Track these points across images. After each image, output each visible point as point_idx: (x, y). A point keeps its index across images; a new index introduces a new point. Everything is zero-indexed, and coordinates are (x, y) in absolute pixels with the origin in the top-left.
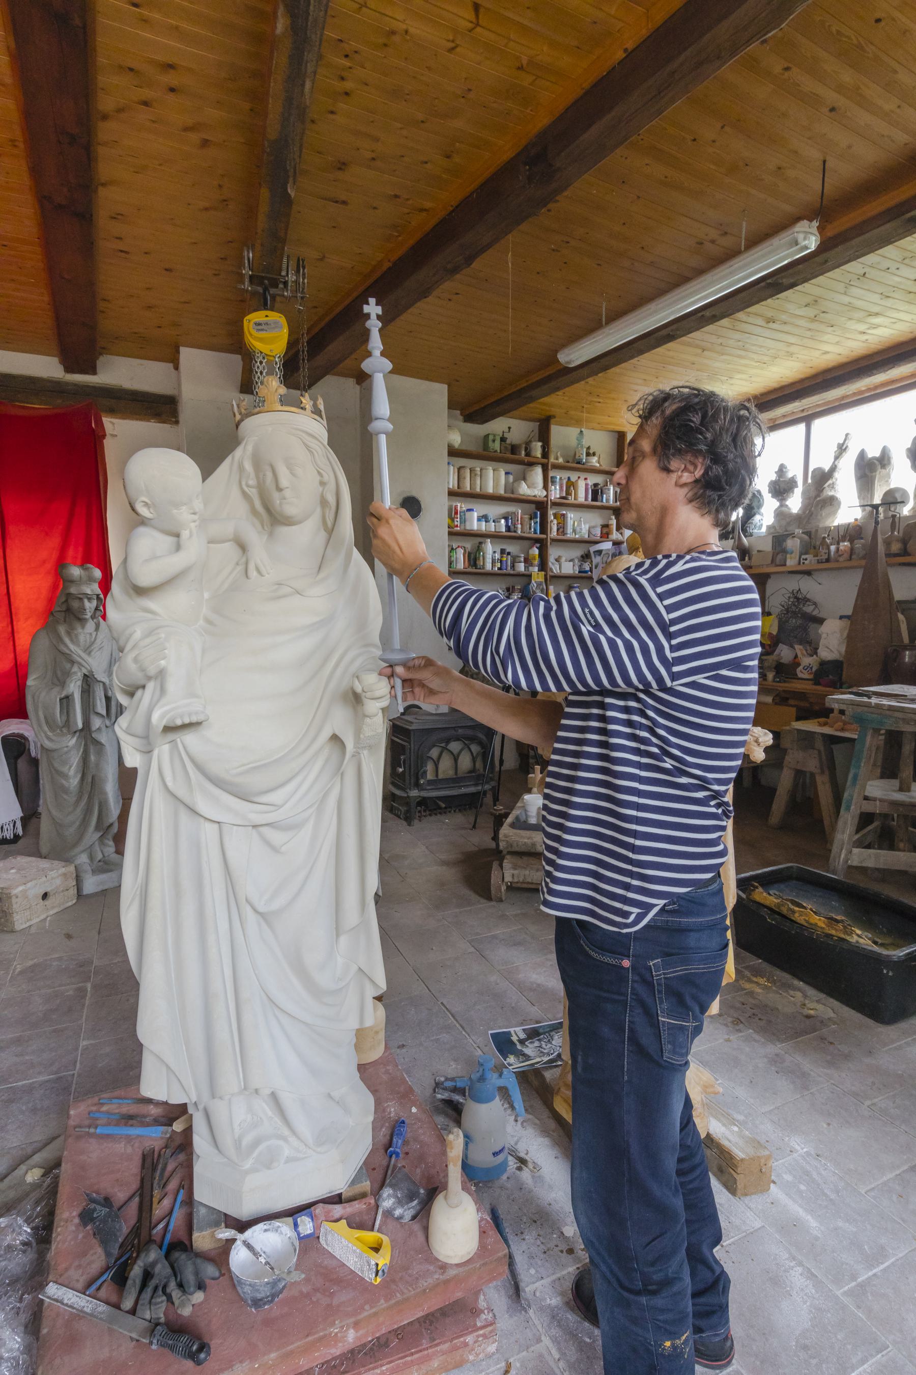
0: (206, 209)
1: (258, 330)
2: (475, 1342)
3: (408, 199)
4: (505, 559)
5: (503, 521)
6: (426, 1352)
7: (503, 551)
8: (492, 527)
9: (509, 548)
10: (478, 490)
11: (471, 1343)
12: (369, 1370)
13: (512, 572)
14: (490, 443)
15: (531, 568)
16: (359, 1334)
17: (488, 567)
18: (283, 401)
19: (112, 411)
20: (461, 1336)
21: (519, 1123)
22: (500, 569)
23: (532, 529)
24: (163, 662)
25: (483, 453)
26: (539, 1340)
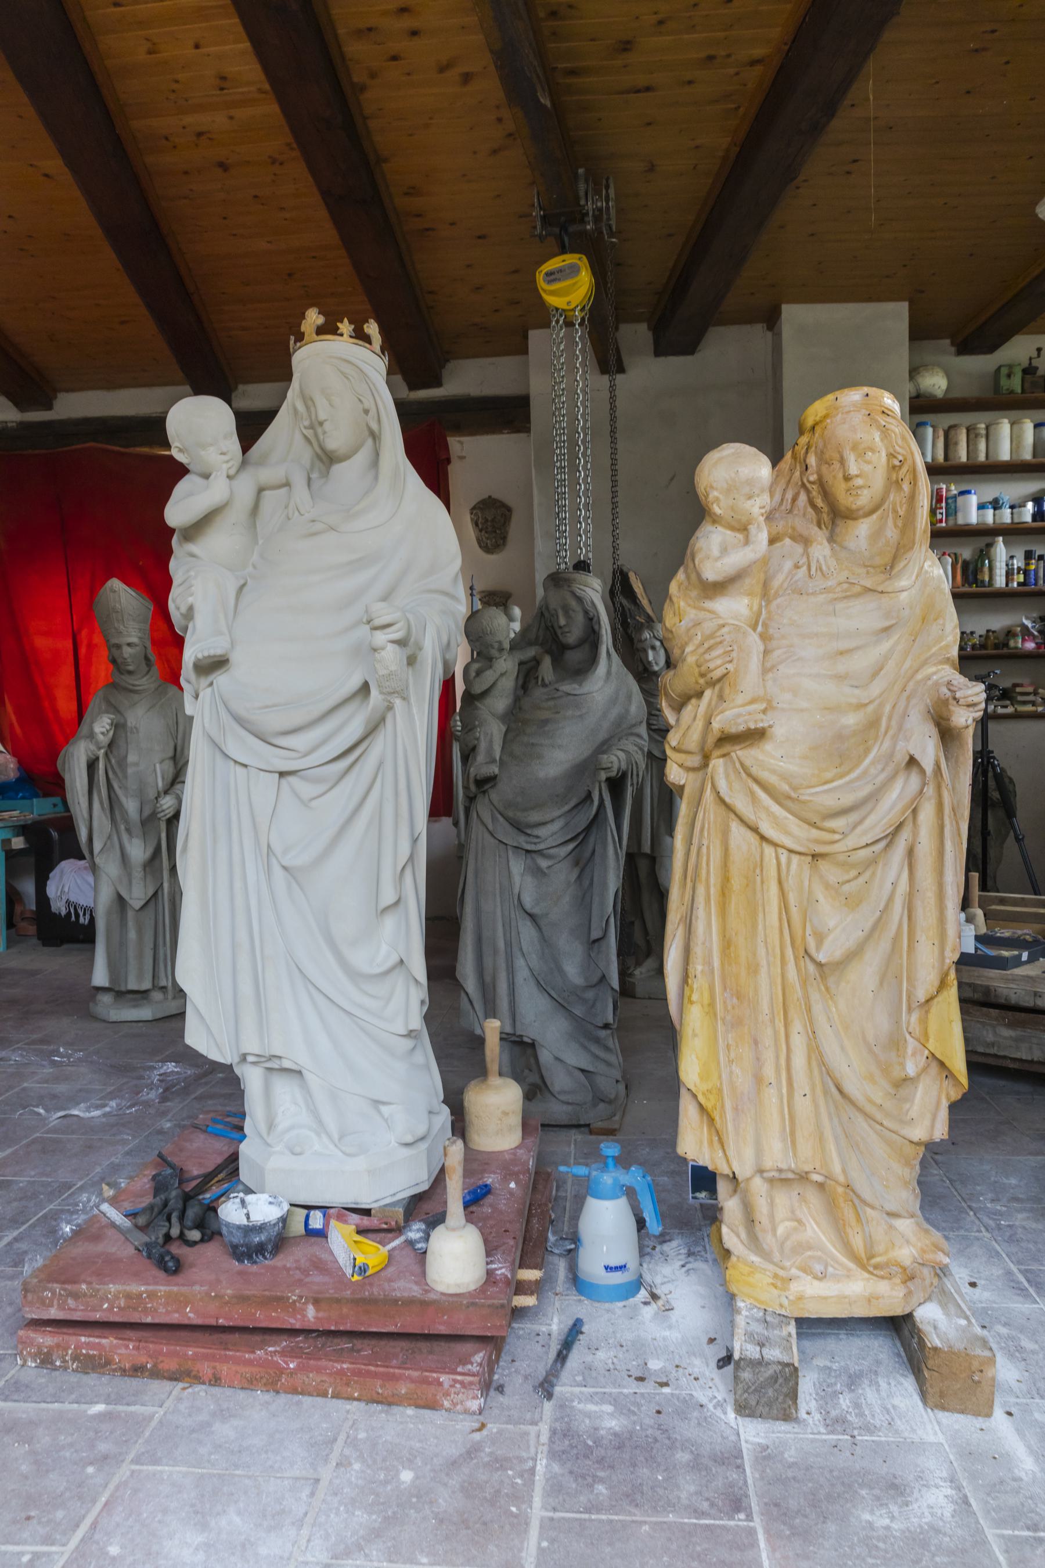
0: (495, 152)
1: (549, 282)
2: (452, 1386)
3: (729, 56)
4: (1033, 567)
5: (1030, 505)
6: (392, 1370)
7: (1028, 555)
8: (1006, 516)
10: (982, 457)
11: (446, 1386)
12: (330, 1360)
14: (1004, 382)
16: (321, 1315)
17: (1000, 582)
18: (321, 331)
19: (459, 429)
20: (435, 1372)
21: (684, 1269)
22: (1019, 584)
24: (190, 600)
25: (996, 400)
26: (534, 1423)
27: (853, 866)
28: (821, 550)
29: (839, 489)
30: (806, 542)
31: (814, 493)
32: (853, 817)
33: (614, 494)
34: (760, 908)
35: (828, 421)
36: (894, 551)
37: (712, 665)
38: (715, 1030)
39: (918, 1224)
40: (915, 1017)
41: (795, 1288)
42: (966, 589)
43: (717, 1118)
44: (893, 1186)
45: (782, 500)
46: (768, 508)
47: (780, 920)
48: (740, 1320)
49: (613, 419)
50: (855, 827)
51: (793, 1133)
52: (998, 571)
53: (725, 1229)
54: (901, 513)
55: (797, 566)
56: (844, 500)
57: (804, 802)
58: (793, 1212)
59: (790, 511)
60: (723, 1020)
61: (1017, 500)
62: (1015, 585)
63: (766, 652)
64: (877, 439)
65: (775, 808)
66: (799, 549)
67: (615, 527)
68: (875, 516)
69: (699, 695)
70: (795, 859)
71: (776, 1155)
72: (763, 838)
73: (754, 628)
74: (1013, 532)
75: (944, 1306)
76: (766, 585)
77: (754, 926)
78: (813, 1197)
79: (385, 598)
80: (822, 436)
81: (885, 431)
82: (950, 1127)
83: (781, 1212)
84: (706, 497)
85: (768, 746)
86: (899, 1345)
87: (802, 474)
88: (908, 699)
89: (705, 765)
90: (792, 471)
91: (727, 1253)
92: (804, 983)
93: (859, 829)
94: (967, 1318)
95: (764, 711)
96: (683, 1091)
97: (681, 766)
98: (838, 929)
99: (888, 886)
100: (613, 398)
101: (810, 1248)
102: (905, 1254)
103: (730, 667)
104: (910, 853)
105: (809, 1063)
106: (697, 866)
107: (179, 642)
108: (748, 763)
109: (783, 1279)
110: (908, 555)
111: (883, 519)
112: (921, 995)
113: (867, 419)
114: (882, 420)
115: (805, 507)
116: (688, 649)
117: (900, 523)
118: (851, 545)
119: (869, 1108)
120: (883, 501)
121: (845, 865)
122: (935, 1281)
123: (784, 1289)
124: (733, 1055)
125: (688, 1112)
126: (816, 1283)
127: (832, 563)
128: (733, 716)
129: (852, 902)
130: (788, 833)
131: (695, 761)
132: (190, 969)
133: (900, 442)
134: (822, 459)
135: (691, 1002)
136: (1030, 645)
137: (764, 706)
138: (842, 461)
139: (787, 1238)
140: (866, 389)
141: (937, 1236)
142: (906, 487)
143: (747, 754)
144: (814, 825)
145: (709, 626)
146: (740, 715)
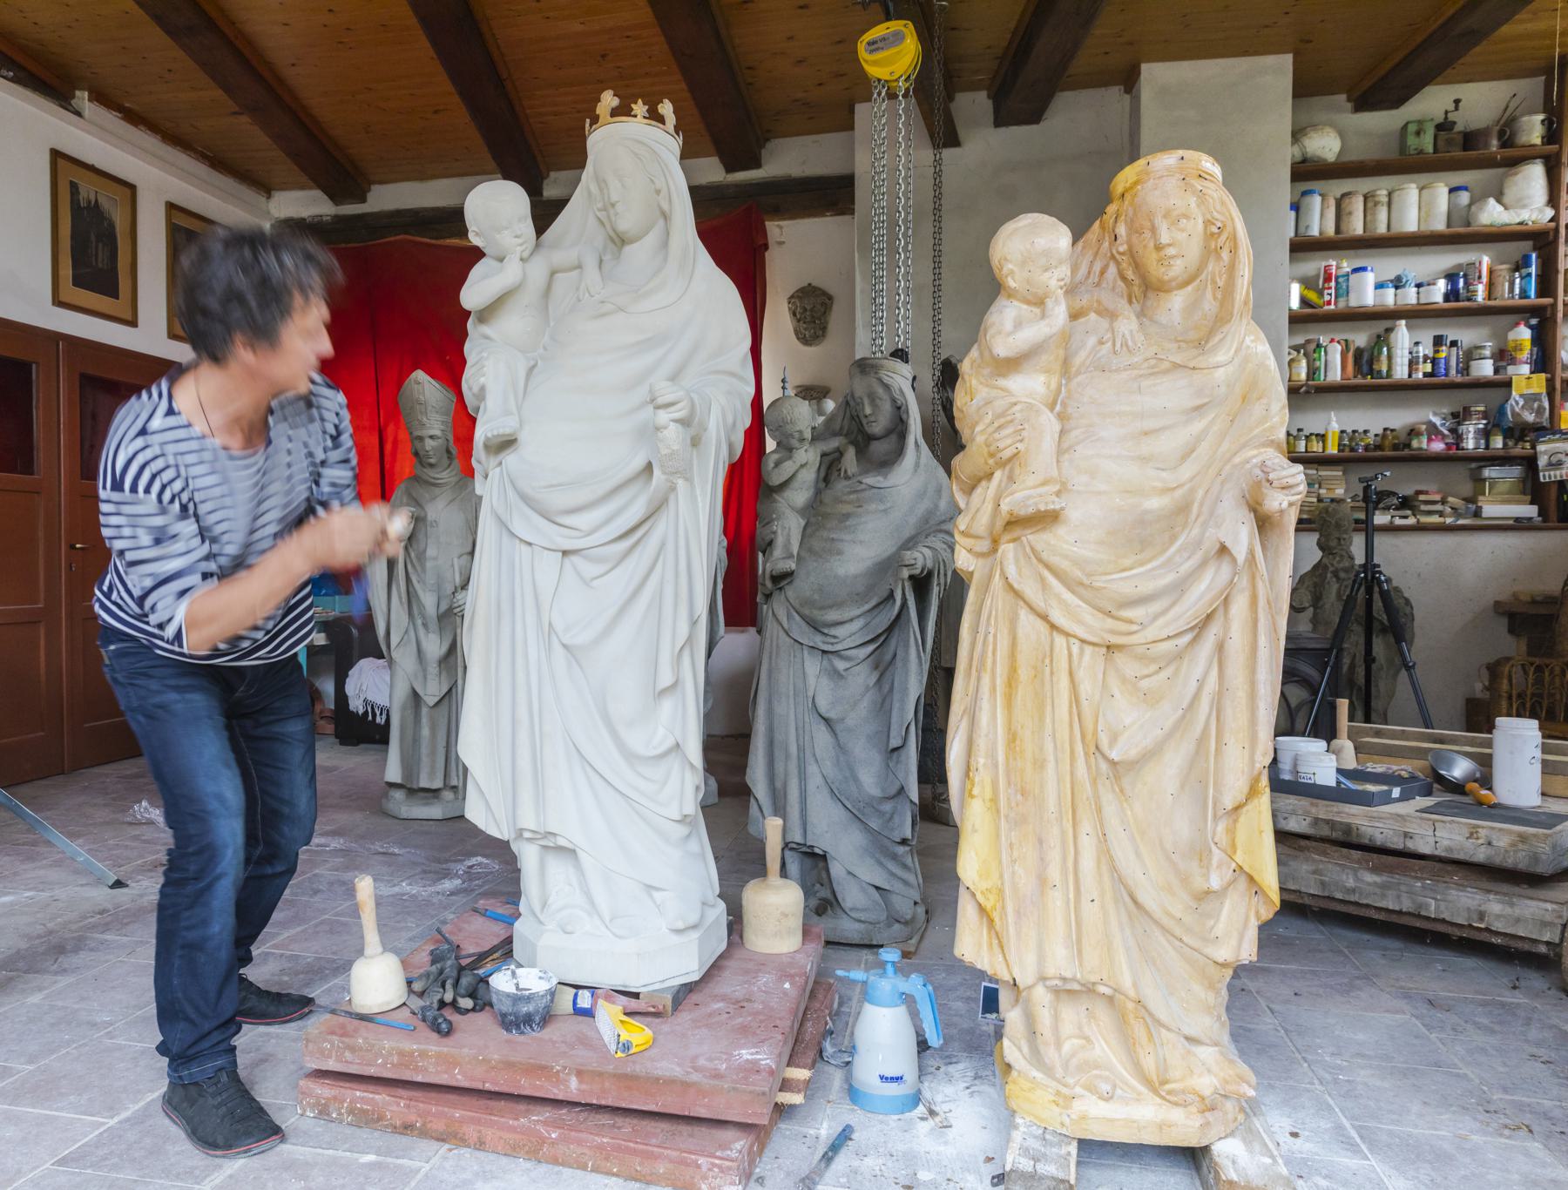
4: (1443, 355)
5: (1442, 285)
7: (1438, 341)
9: (1451, 334)
13: (1459, 379)
15: (1511, 370)
22: (1426, 375)
23: (1519, 288)
27: (1153, 660)
28: (1128, 324)
29: (1151, 259)
30: (1112, 315)
31: (1124, 265)
32: (1155, 607)
33: (937, 276)
34: (1049, 701)
37: (1001, 445)
38: (998, 829)
39: (1222, 1053)
40: (1221, 827)
41: (1078, 1106)
42: (1359, 381)
43: (997, 920)
44: (1196, 1010)
46: (1068, 280)
47: (1071, 713)
48: (1017, 1136)
49: (938, 197)
50: (1156, 617)
51: (1079, 941)
52: (1399, 360)
53: (1006, 1042)
54: (1220, 284)
55: (1101, 343)
56: (1155, 271)
57: (1098, 589)
58: (1080, 1028)
59: (1098, 285)
60: (1006, 817)
61: (1426, 278)
62: (1420, 375)
63: (1062, 432)
64: (1193, 205)
65: (1068, 596)
66: (1105, 323)
67: (936, 311)
68: (1190, 288)
69: (989, 476)
70: (1088, 650)
71: (1060, 962)
72: (1053, 627)
73: (1052, 408)
74: (1418, 315)
75: (1248, 1143)
76: (1066, 363)
77: (1042, 719)
78: (1103, 1014)
79: (674, 378)
82: (1260, 947)
83: (1067, 1028)
84: (1001, 270)
85: (1061, 531)
86: (1198, 1183)
88: (1222, 483)
89: (994, 550)
91: (1009, 1066)
92: (1094, 782)
93: (1161, 621)
94: (1272, 1157)
95: (1058, 494)
96: (962, 890)
97: (970, 551)
98: (1131, 724)
99: (1193, 685)
100: (938, 174)
101: (1097, 1067)
102: (1206, 1084)
103: (1019, 446)
104: (1220, 648)
105: (1099, 867)
106: (984, 652)
107: (473, 420)
108: (1039, 548)
109: (1065, 1097)
110: (1225, 330)
112: (1229, 803)
113: (1182, 184)
116: (978, 429)
119: (1165, 921)
120: (1199, 271)
121: (1144, 659)
122: (1241, 1117)
123: (1066, 1108)
124: (1016, 854)
125: (967, 913)
126: (1101, 1103)
127: (1140, 338)
128: (1025, 496)
129: (1149, 699)
130: (1081, 622)
131: (984, 546)
132: (472, 746)
134: (1134, 230)
135: (972, 796)
136: (1438, 446)
137: (1057, 487)
138: (1153, 230)
139: (1073, 1055)
141: (1244, 1069)
142: (1225, 255)
143: (1038, 539)
144: (1109, 614)
145: (1000, 405)
146: (1029, 498)
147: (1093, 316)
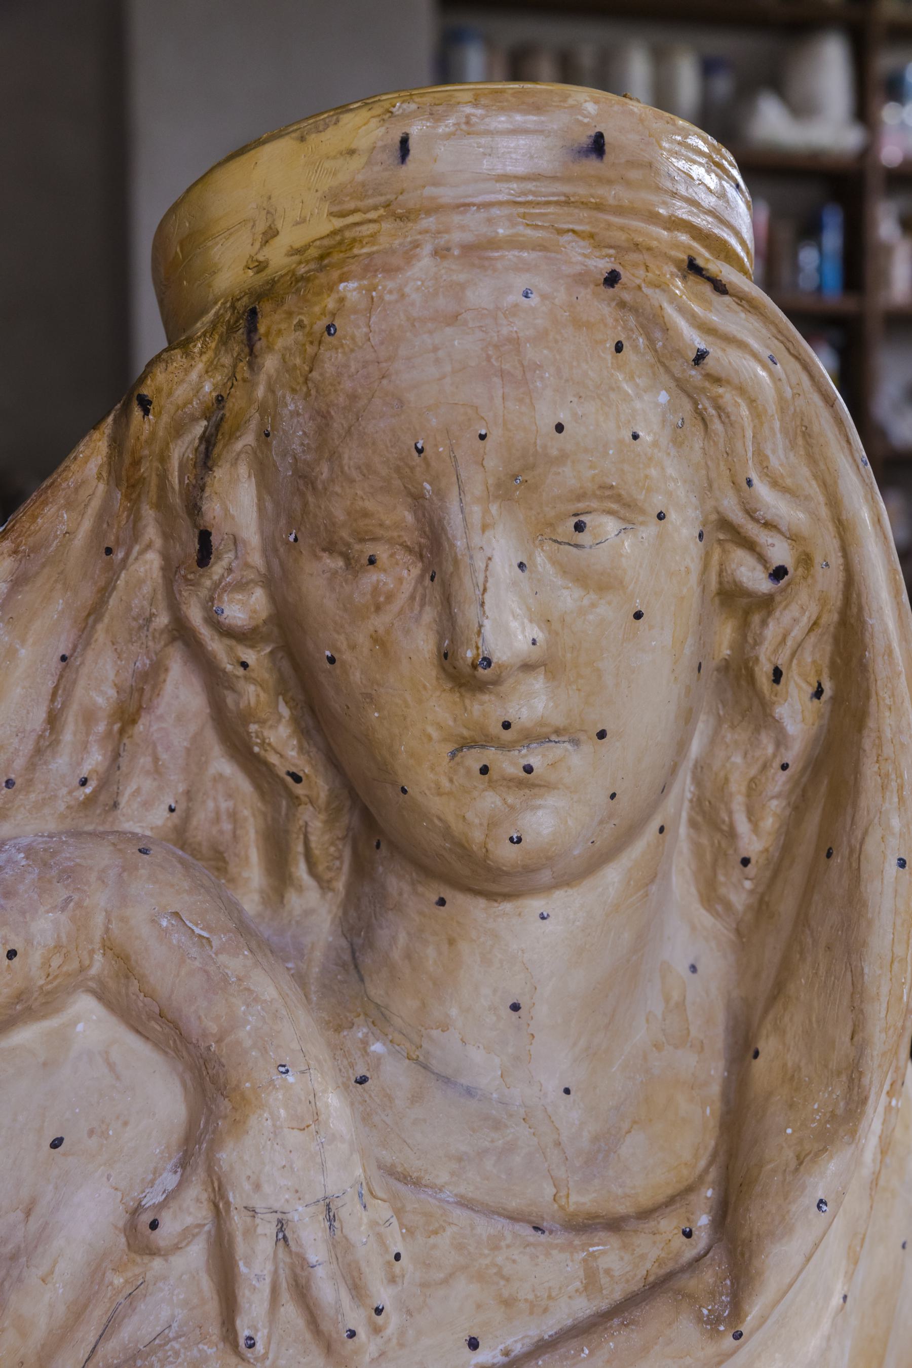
31: (251, 694)
35: (350, 289)
36: (715, 1071)
45: (53, 720)
54: (752, 843)
59: (101, 796)
68: (613, 876)
80: (305, 377)
81: (697, 381)
87: (171, 570)
90: (108, 552)
110: (825, 1177)
111: (652, 876)
113: (599, 307)
114: (687, 315)
115: (195, 756)
117: (739, 893)
118: (482, 1065)
133: (779, 456)
138: (435, 556)
140: (587, 105)
147: (88, 1021)
